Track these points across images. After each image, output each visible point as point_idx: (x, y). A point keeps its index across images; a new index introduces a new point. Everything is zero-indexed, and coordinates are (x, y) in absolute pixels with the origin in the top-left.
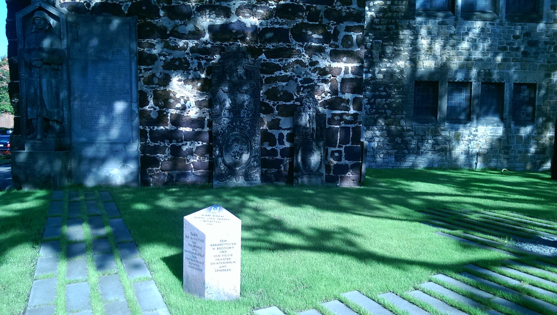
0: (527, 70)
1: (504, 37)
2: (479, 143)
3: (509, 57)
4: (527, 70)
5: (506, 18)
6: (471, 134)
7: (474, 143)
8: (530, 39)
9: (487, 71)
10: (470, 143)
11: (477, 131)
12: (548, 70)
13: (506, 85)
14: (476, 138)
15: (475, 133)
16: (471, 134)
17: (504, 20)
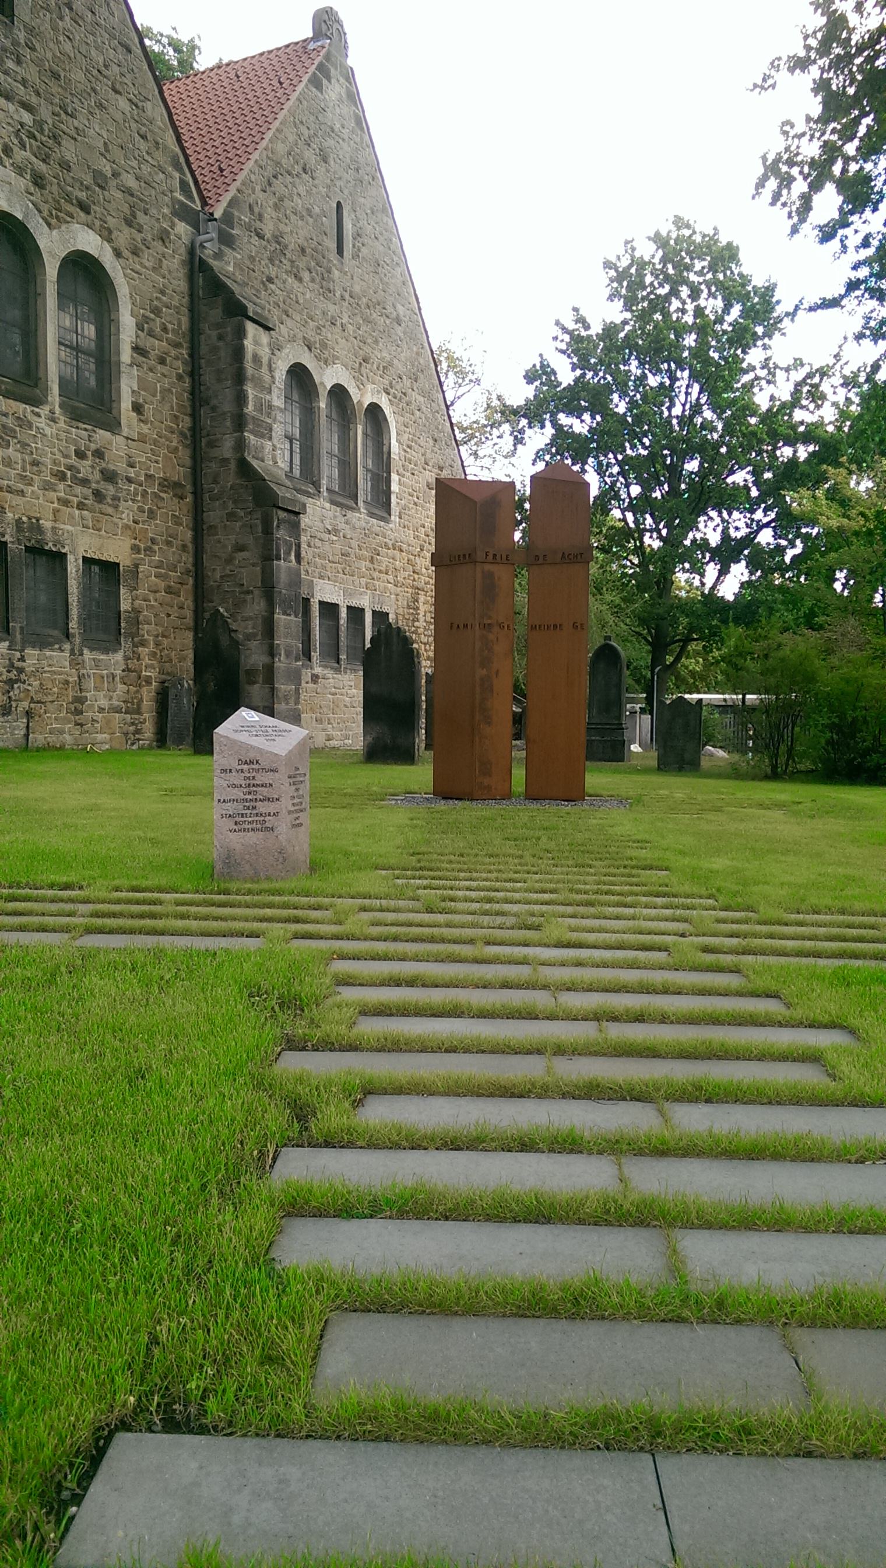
0: (103, 533)
1: (59, 450)
2: (30, 688)
3: (72, 498)
4: (103, 533)
5: (60, 406)
6: (12, 665)
7: (19, 688)
8: (104, 465)
9: (34, 521)
10: (13, 688)
11: (22, 659)
12: (136, 539)
13: (70, 558)
14: (23, 677)
15: (20, 664)
16: (13, 666)
17: (57, 410)
